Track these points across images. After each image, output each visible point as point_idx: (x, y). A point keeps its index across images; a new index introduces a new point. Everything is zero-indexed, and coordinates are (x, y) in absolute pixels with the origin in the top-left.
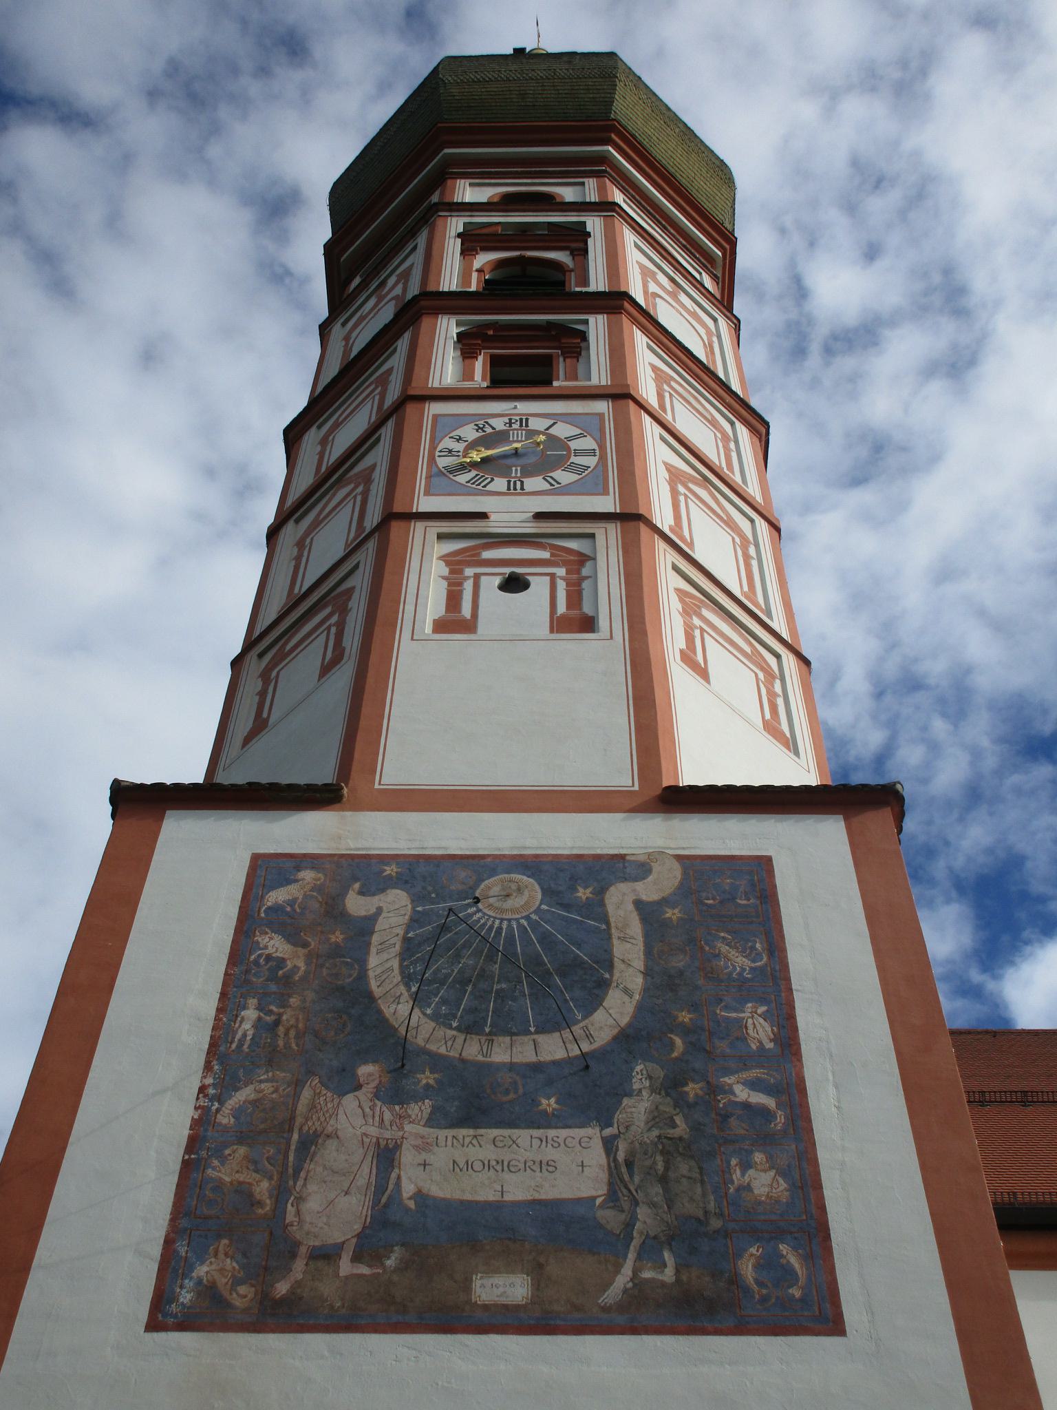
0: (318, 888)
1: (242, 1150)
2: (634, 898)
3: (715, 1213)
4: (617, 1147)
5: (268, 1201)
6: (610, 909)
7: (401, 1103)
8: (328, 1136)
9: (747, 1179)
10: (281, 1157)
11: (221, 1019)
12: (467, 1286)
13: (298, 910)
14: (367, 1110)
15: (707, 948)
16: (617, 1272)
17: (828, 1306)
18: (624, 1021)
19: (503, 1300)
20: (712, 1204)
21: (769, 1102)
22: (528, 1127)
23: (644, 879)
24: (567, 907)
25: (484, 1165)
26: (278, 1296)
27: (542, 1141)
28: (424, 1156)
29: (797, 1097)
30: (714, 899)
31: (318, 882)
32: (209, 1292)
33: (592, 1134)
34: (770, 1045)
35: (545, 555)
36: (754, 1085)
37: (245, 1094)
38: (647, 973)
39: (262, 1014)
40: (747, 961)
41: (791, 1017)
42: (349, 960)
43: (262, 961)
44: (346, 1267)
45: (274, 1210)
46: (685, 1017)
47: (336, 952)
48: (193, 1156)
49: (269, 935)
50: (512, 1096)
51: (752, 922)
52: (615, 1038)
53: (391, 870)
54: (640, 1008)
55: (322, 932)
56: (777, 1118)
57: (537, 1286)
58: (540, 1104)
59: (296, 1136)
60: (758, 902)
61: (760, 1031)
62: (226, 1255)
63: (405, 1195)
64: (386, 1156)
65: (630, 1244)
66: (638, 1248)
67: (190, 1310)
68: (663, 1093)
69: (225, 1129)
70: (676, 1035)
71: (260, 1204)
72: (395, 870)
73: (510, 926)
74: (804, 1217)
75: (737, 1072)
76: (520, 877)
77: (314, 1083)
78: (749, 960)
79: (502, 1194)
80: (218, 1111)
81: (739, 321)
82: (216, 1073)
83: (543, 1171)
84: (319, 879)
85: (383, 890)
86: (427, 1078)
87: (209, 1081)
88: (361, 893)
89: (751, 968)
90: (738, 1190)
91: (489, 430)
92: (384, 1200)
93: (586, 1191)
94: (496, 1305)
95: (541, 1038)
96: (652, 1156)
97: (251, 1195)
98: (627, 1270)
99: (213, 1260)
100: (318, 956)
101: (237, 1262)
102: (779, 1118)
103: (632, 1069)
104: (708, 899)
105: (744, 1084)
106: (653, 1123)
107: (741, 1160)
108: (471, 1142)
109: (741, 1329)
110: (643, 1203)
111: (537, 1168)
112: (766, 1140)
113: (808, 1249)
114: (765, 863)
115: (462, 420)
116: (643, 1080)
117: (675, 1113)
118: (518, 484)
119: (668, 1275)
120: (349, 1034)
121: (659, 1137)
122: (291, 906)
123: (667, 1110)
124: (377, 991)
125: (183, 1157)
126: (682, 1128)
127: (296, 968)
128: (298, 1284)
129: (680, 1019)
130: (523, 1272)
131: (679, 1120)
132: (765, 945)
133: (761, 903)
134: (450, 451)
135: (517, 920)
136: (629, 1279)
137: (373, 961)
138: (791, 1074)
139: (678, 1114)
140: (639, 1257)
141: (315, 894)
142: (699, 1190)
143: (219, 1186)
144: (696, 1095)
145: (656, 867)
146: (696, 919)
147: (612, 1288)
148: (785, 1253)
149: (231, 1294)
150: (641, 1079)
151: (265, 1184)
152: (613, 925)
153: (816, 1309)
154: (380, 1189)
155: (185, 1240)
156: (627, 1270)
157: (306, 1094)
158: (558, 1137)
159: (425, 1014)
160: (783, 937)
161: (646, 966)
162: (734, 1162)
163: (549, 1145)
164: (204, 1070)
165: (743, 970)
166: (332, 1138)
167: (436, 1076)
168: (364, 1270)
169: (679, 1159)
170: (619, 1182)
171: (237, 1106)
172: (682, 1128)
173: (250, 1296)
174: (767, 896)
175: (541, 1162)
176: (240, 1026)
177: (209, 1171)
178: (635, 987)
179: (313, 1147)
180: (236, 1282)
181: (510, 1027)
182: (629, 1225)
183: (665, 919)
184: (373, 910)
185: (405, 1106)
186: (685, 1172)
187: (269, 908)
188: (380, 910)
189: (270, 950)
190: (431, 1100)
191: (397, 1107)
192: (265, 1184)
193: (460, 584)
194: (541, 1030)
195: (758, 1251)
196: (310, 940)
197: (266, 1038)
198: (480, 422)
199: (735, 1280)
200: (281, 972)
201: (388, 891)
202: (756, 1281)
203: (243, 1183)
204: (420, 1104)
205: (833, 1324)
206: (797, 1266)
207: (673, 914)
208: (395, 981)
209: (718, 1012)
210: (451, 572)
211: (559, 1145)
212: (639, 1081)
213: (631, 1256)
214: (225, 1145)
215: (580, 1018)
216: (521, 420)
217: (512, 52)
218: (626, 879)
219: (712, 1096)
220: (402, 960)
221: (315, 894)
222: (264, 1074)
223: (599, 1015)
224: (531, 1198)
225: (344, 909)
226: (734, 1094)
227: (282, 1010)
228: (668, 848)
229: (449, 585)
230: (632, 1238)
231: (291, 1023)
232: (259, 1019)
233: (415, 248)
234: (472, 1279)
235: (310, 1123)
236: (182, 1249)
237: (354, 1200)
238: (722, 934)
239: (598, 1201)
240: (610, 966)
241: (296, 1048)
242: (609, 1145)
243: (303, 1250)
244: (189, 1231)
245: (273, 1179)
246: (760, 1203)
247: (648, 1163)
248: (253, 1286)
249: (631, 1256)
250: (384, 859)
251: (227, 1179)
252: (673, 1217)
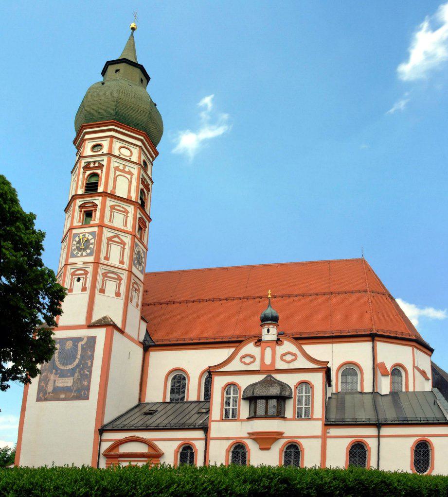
33: (72, 378)
36: (87, 371)
44: (51, 394)
61: (89, 364)
64: (55, 382)
86: (59, 371)
174: (95, 343)
181: (67, 365)
212: (77, 371)
242: (73, 379)
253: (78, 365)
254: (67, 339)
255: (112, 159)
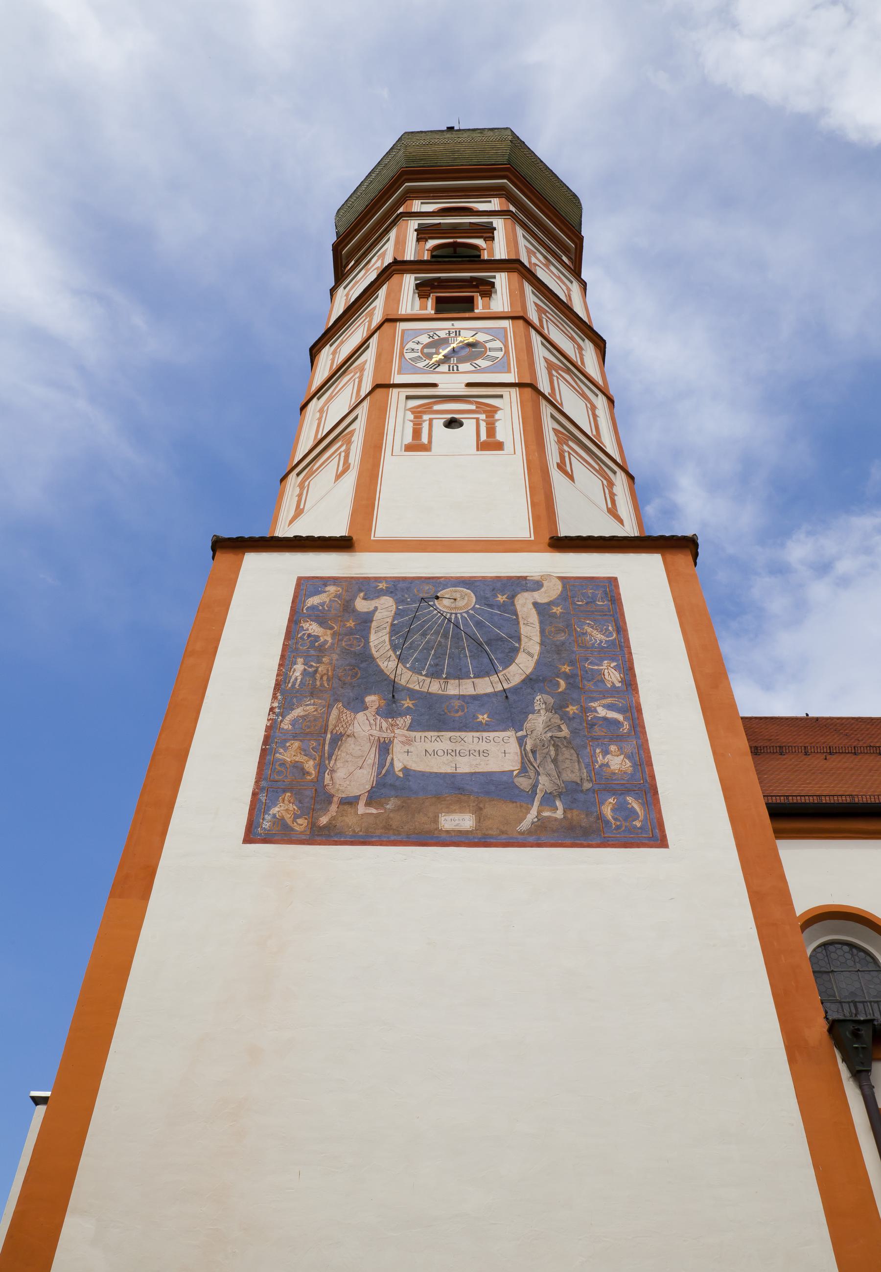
0: (338, 596)
1: (297, 744)
2: (533, 601)
3: (587, 780)
4: (526, 742)
5: (313, 772)
6: (518, 608)
7: (393, 718)
8: (348, 736)
9: (606, 760)
10: (321, 747)
11: (282, 670)
12: (436, 820)
13: (326, 609)
14: (372, 722)
15: (579, 630)
16: (528, 812)
17: (657, 831)
18: (528, 671)
19: (458, 828)
20: (585, 774)
21: (620, 717)
22: (471, 731)
23: (538, 590)
24: (490, 606)
25: (444, 752)
26: (321, 825)
27: (479, 739)
28: (407, 748)
29: (636, 713)
30: (582, 601)
31: (338, 593)
32: (280, 822)
33: (509, 736)
34: (620, 685)
35: (473, 407)
36: (609, 707)
37: (298, 712)
38: (542, 644)
39: (306, 667)
40: (603, 637)
41: (631, 669)
42: (358, 637)
43: (305, 637)
44: (362, 809)
45: (317, 777)
46: (566, 669)
47: (350, 632)
48: (267, 747)
49: (309, 623)
50: (460, 713)
51: (606, 615)
52: (523, 681)
53: (382, 586)
54: (538, 663)
55: (341, 621)
56: (624, 726)
57: (479, 820)
58: (478, 718)
59: (329, 736)
60: (610, 603)
61: (613, 676)
62: (290, 802)
63: (396, 769)
64: (384, 748)
65: (535, 797)
66: (540, 799)
67: (269, 832)
68: (553, 711)
69: (286, 732)
70: (561, 679)
71: (308, 773)
72: (385, 585)
73: (456, 617)
74: (642, 782)
75: (598, 700)
76: (462, 589)
77: (339, 706)
78: (605, 636)
79: (456, 768)
80: (281, 721)
81: (586, 283)
82: (280, 701)
83: (481, 755)
84: (339, 591)
85: (378, 597)
87: (276, 704)
88: (365, 599)
89: (606, 641)
90: (600, 767)
91: (436, 337)
92: (384, 772)
93: (507, 768)
94: (454, 831)
95: (476, 681)
96: (547, 748)
97: (303, 769)
98: (534, 812)
99: (281, 804)
100: (340, 635)
101: (296, 805)
102: (625, 726)
103: (534, 699)
104: (579, 601)
105: (603, 707)
106: (547, 729)
107: (602, 749)
108: (436, 739)
109: (604, 844)
110: (543, 774)
111: (476, 754)
112: (618, 738)
113: (645, 799)
114: (613, 582)
115: (420, 332)
116: (541, 704)
117: (561, 723)
118: (455, 367)
119: (559, 814)
120: (358, 679)
121: (551, 737)
122: (322, 606)
123: (556, 721)
124: (376, 655)
125: (262, 747)
126: (565, 732)
127: (326, 642)
128: (333, 818)
129: (563, 670)
130: (470, 813)
131: (563, 727)
132: (615, 628)
133: (612, 604)
134: (413, 350)
135: (461, 614)
136: (535, 817)
137: (373, 637)
138: (632, 701)
139: (563, 724)
140: (541, 804)
141: (336, 599)
142: (577, 767)
143: (283, 764)
144: (574, 713)
145: (545, 583)
146: (572, 613)
147: (525, 821)
148: (630, 802)
149: (293, 824)
150: (540, 704)
151: (311, 763)
152: (520, 617)
153: (651, 833)
154: (381, 765)
155: (264, 793)
156: (534, 812)
157: (334, 713)
158: (489, 737)
159: (405, 667)
160: (625, 623)
161: (541, 640)
162: (598, 751)
163: (484, 741)
164: (272, 699)
165: (601, 642)
166: (351, 737)
167: (413, 702)
168: (374, 811)
169: (564, 749)
170: (527, 762)
171: (293, 719)
172: (565, 732)
173: (305, 824)
175: (479, 750)
176: (293, 674)
177: (277, 755)
178: (535, 652)
179: (340, 742)
180: (296, 817)
181: (460, 674)
182: (535, 786)
183: (552, 613)
184: (372, 608)
185: (395, 719)
186: (568, 756)
187: (308, 608)
188: (376, 608)
189: (310, 631)
190: (410, 716)
191: (390, 720)
192: (311, 763)
193: (421, 424)
194: (477, 676)
195: (614, 801)
196: (333, 625)
197: (309, 680)
198: (431, 333)
199: (600, 817)
200: (317, 644)
201: (381, 598)
202: (612, 817)
203: (297, 762)
204: (404, 718)
205: (661, 841)
206: (638, 809)
207: (557, 610)
208: (387, 648)
209: (586, 666)
210: (415, 417)
211: (490, 741)
213: (536, 803)
214: (286, 741)
215: (501, 669)
216: (456, 332)
217: (446, 129)
218: (527, 590)
219: (584, 714)
220: (391, 636)
221: (336, 599)
222: (308, 701)
223: (513, 668)
224: (474, 771)
225: (354, 608)
226: (596, 712)
227: (318, 665)
228: (553, 572)
229: (414, 424)
230: (536, 794)
231: (324, 672)
232: (305, 670)
233: (388, 240)
234: (439, 817)
235: (337, 729)
236: (263, 797)
237: (365, 772)
238: (588, 622)
239: (515, 773)
240: (519, 640)
241: (328, 686)
242: (521, 741)
243: (335, 799)
244: (266, 789)
245: (316, 760)
246: (614, 774)
247: (546, 751)
248: (306, 819)
249: (536, 803)
250: (378, 579)
251: (289, 760)
252: (562, 782)
253: (531, 682)
254: (439, 582)
255: (433, 312)
